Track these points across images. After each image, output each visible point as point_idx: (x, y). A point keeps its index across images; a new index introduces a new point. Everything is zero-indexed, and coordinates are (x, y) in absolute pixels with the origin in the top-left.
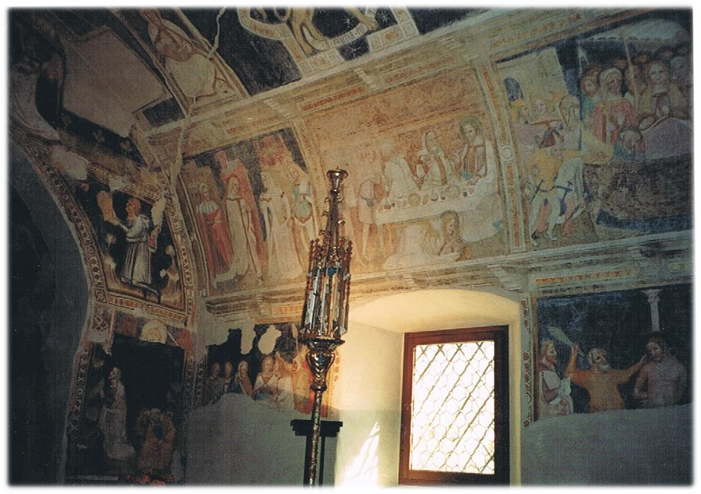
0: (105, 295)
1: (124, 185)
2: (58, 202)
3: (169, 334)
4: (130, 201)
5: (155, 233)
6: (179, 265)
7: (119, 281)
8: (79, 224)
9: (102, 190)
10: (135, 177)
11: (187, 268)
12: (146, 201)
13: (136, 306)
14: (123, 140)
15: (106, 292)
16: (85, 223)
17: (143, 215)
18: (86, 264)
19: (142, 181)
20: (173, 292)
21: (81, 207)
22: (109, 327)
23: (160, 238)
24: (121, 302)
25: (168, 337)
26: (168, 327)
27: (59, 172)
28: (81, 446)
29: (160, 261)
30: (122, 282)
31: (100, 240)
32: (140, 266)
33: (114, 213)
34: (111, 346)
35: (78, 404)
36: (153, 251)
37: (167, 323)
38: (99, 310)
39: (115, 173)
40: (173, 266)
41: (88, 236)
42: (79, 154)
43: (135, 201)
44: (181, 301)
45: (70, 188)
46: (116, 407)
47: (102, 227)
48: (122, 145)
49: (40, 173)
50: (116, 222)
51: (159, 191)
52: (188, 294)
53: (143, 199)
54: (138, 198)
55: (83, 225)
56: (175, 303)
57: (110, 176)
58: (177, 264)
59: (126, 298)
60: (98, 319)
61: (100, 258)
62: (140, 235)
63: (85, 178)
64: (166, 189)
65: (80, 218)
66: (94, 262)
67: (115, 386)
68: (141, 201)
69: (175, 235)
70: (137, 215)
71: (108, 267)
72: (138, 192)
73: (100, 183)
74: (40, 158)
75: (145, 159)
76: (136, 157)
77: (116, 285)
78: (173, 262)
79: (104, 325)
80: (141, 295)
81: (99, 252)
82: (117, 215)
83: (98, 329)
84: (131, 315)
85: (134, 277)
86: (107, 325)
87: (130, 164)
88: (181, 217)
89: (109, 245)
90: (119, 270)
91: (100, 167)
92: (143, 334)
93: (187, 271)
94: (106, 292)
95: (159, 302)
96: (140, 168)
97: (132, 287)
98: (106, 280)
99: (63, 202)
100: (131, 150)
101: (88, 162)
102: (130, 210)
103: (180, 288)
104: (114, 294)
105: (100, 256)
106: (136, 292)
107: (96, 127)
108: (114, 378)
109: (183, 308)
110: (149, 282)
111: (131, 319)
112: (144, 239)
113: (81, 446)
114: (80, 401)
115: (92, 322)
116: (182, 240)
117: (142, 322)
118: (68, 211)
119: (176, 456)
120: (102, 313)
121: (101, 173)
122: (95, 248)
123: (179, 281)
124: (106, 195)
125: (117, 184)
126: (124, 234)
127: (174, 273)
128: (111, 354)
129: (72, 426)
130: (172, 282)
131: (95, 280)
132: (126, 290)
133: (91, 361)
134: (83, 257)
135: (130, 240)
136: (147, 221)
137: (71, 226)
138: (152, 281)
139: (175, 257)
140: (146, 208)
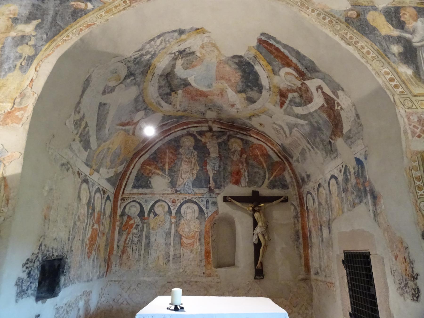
0: (411, 101)
2: (331, 34)
4: (402, 12)
8: (359, 45)
9: (369, 11)
12: (419, 6)
15: (414, 99)
16: (363, 42)
21: (355, 31)
27: (323, 10)
31: (385, 53)
33: (390, 26)
38: (411, 117)
41: (372, 53)
43: (408, 10)
47: (382, 44)
49: (307, 16)
50: (396, 33)
53: (416, 5)
54: (410, 7)
55: (363, 44)
60: (414, 126)
61: (392, 67)
63: (349, 7)
65: (357, 40)
66: (388, 74)
68: (415, 8)
70: (416, 21)
71: (404, 75)
73: (366, 6)
74: (302, 5)
77: (421, 89)
81: (389, 63)
82: (394, 27)
83: (419, 136)
89: (397, 55)
98: (408, 88)
99: (336, 32)
102: (405, 18)
105: (392, 67)
115: (409, 131)
118: (343, 38)
120: (416, 120)
122: (383, 60)
124: (376, 13)
131: (396, 90)
134: (373, 73)
135: (419, 44)
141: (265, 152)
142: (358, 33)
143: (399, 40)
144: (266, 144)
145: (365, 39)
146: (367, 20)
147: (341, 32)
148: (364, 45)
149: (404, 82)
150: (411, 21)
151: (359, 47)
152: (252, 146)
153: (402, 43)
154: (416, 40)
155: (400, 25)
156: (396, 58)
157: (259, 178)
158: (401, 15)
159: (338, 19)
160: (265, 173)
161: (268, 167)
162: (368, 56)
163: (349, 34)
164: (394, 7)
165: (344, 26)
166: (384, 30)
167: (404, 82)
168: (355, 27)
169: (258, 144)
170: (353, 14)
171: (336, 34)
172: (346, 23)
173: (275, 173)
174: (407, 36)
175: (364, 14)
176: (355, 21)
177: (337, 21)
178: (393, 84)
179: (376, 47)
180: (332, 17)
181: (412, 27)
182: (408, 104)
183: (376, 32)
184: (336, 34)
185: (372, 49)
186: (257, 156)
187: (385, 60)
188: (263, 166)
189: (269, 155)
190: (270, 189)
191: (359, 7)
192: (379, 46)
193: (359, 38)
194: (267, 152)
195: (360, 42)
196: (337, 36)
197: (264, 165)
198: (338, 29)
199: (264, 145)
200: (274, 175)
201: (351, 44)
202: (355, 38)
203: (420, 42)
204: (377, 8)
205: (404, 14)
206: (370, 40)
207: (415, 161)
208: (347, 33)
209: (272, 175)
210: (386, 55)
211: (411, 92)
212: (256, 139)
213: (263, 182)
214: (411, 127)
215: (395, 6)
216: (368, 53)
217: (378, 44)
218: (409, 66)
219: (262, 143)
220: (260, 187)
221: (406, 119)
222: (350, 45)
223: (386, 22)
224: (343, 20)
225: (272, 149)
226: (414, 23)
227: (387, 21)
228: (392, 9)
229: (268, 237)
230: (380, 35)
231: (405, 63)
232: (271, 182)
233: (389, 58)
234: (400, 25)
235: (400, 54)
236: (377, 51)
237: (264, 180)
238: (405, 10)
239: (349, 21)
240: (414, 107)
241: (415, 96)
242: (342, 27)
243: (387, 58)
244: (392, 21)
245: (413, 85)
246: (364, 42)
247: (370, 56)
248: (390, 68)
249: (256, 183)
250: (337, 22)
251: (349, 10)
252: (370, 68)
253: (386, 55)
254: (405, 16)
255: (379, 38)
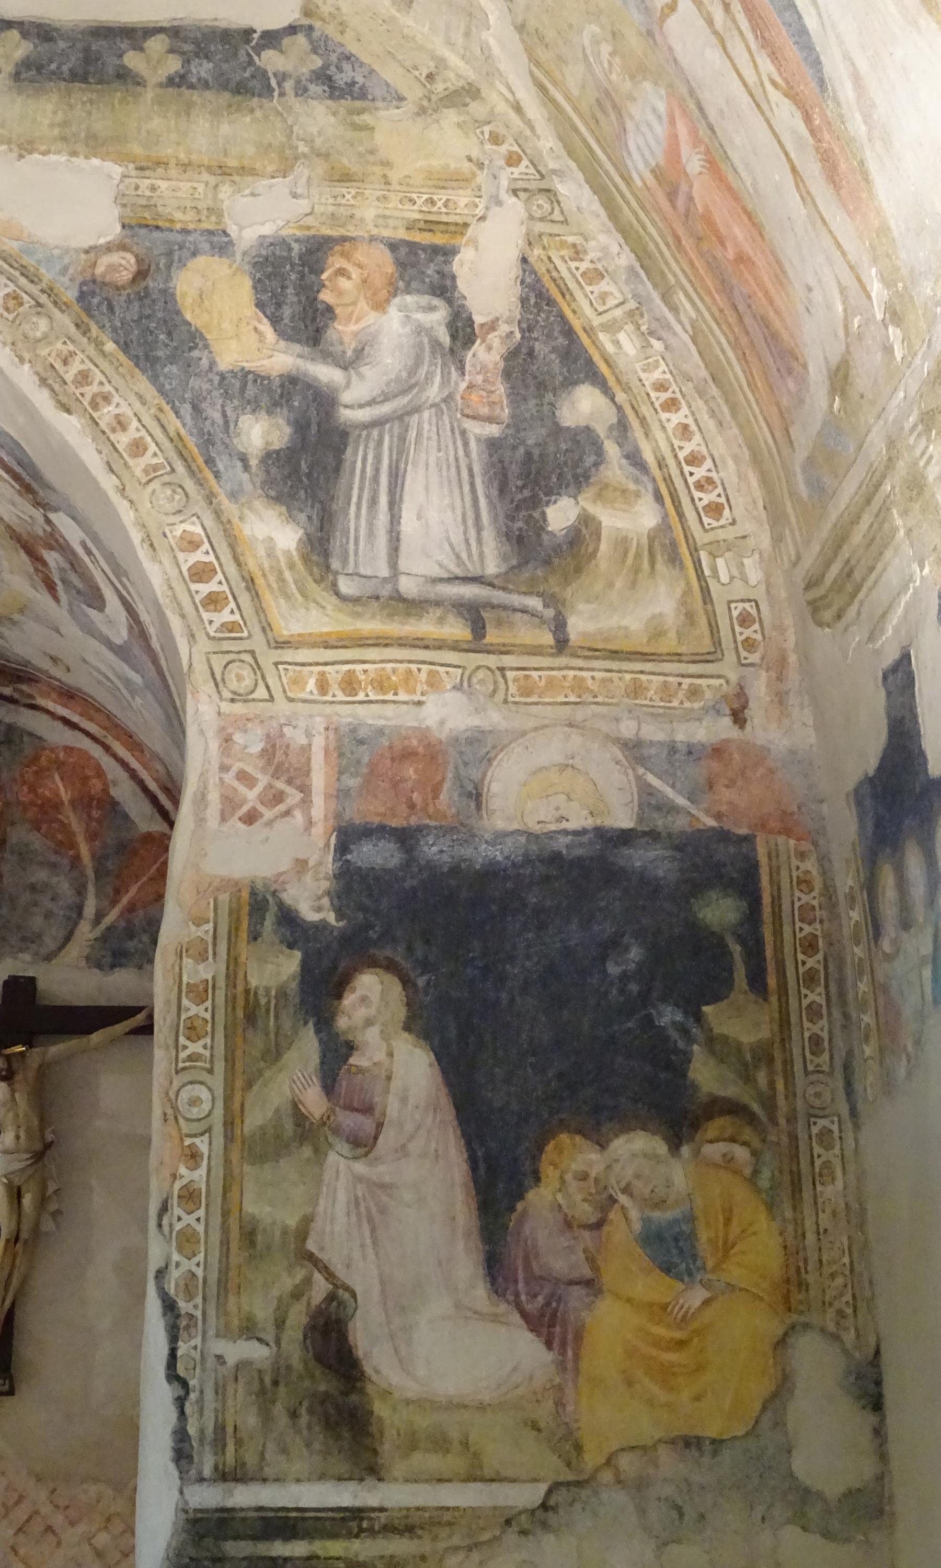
0: (257, 666)
1: (303, 205)
3: (651, 779)
4: (336, 262)
5: (487, 355)
6: (649, 457)
7: (330, 601)
8: (106, 414)
9: (194, 254)
10: (348, 162)
11: (694, 460)
13: (434, 683)
14: (271, 39)
16: (132, 401)
17: (409, 299)
18: (155, 558)
19: (386, 164)
20: (634, 584)
21: (110, 346)
22: (306, 802)
23: (519, 365)
24: (350, 684)
25: (646, 790)
26: (634, 750)
28: (237, 1351)
29: (530, 474)
30: (356, 600)
31: (206, 452)
32: (433, 515)
33: (266, 327)
34: (325, 885)
35: (193, 1156)
36: (493, 430)
37: (627, 729)
38: (238, 738)
39: (253, 172)
40: (615, 467)
41: (153, 448)
42: (74, 154)
43: (359, 255)
44: (690, 616)
45: (49, 291)
46: (402, 1151)
48: (270, 60)
51: (482, 178)
52: (724, 577)
53: (402, 234)
54: (373, 239)
55: (125, 409)
56: (658, 633)
57: (225, 191)
58: (634, 459)
59: (370, 664)
60: (243, 776)
61: (218, 514)
62: (407, 385)
63: (115, 231)
64: (512, 160)
65: (107, 388)
66: (192, 544)
67: (380, 1056)
68: (393, 246)
69: (603, 337)
70: (380, 306)
71: (262, 552)
72: (378, 214)
73: (185, 231)
75: (391, 74)
76: (341, 82)
77: (314, 613)
78: (612, 449)
79: (279, 797)
80: (457, 630)
81: (210, 498)
82: (281, 334)
84: (423, 733)
85: (404, 564)
86: (294, 796)
87: (318, 118)
88: (625, 259)
89: (254, 462)
90: (320, 549)
91: (173, 172)
92: (495, 804)
93: (700, 473)
94: (268, 658)
95: (562, 644)
96: (366, 118)
97: (411, 606)
98: (260, 609)
100: (318, 62)
101: (117, 170)
102: (340, 293)
103: (674, 559)
104: (304, 655)
106: (425, 627)
107: (136, 35)
108: (369, 1023)
109: (706, 645)
110: (492, 568)
111: (424, 753)
112: (434, 392)
113: (237, 1351)
114: (202, 1145)
115: (214, 796)
116: (647, 346)
117: (480, 748)
119: (817, 1366)
121: (176, 195)
122: (189, 485)
123: (665, 526)
125: (264, 213)
126: (324, 400)
127: (627, 497)
128: (331, 918)
129: (176, 1257)
130: (622, 544)
131: (206, 616)
132: (371, 626)
133: (233, 962)
134: (136, 536)
136: (436, 318)
137: (70, 428)
138: (505, 558)
139: (622, 428)
140: (423, 263)
141: (96, 785)
142: (122, 357)
143: (288, 392)
144: (107, 748)
145: (143, 384)
146: (173, 295)
147: (44, 352)
148: (130, 413)
149: (250, 583)
150: (363, 305)
151: (103, 425)
152: (36, 759)
153: (291, 408)
154: (357, 396)
155: (309, 323)
156: (245, 477)
157: (48, 915)
158: (324, 276)
159: (49, 291)
160: (81, 891)
161: (99, 860)
162: (131, 462)
163: (80, 356)
164: (309, 239)
165: (65, 321)
166: (233, 344)
167: (250, 583)
168: (114, 329)
169: (69, 750)
170: (124, 265)
171: (22, 360)
172: (77, 308)
173: (133, 891)
174: (325, 373)
175: (169, 267)
176: (119, 301)
177: (43, 299)
178: (204, 589)
179: (174, 424)
180: (23, 281)
181: (356, 334)
182: (241, 678)
183: (196, 354)
184: (22, 360)
185: (158, 433)
186: (57, 806)
187: (200, 483)
188: (77, 858)
189: (114, 804)
190: (99, 966)
191: (156, 234)
192: (188, 419)
193: (116, 379)
194: (106, 791)
195: (116, 399)
196: (27, 366)
197: (84, 850)
198: (39, 334)
199: (96, 751)
200: (125, 900)
201: (73, 405)
202: (99, 377)
203: (372, 403)
204: (231, 243)
205: (342, 272)
206: (161, 391)
207: (199, 921)
208: (72, 354)
209: (114, 903)
210: (210, 462)
211: (266, 628)
212: (59, 725)
213: (68, 939)
214: (229, 778)
215: (312, 232)
216: (138, 448)
217: (186, 410)
218: (291, 518)
219: (86, 744)
220: (48, 958)
221: (214, 746)
222: (68, 411)
223: (250, 310)
224: (71, 295)
225: (133, 775)
226: (372, 317)
227: (260, 305)
228: (296, 246)
229: (42, 1201)
230: (212, 364)
231: (278, 499)
232: (103, 939)
233: (217, 475)
234: (309, 323)
235: (269, 457)
236: (177, 441)
237: (76, 924)
238: (346, 255)
239: (95, 301)
240: (261, 692)
241: (282, 645)
242: (54, 328)
243: (210, 476)
244: (279, 305)
245: (288, 597)
246: (133, 399)
247: (138, 465)
248: (209, 522)
249: (30, 940)
250: (39, 305)
251: (108, 248)
252: (127, 516)
253: (210, 462)
254: (344, 283)
255: (194, 383)
